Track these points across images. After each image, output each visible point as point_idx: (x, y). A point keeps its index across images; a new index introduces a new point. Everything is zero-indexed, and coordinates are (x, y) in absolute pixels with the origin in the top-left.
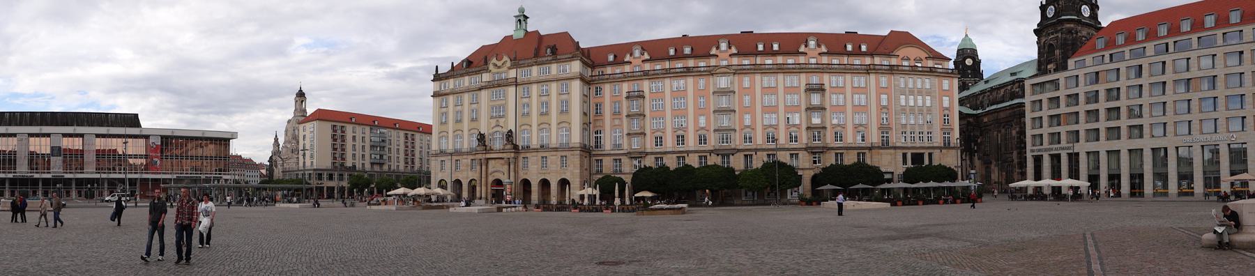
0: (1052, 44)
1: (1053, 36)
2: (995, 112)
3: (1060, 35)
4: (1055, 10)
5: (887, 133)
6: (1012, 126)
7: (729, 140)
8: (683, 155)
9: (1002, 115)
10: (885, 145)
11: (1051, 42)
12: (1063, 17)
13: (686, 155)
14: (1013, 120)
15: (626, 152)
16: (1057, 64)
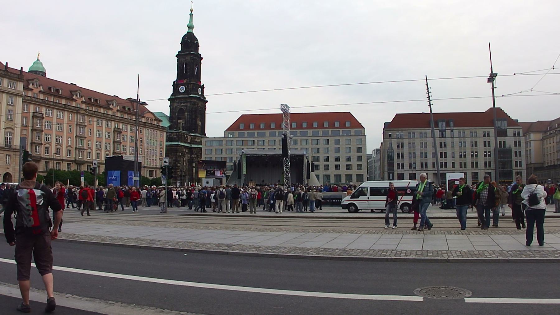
1: (184, 104)
3: (189, 104)
4: (186, 89)
7: (82, 155)
11: (182, 107)
12: (192, 95)
16: (185, 121)
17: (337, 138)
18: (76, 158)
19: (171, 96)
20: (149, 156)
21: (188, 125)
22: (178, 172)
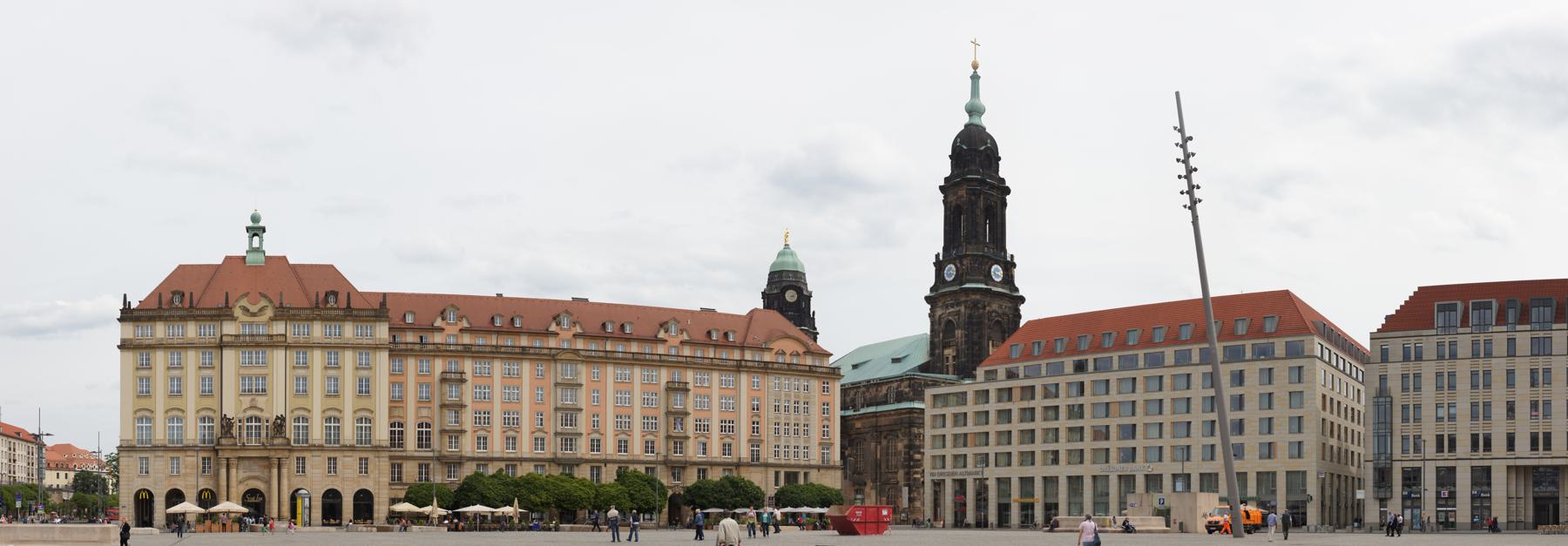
0: (950, 321)
1: (952, 310)
2: (873, 417)
3: (962, 309)
4: (957, 271)
5: (758, 446)
6: (898, 437)
8: (515, 463)
9: (883, 421)
10: (756, 462)
11: (950, 318)
12: (967, 286)
13: (518, 464)
14: (900, 430)
15: (436, 454)
16: (958, 351)
17: (1237, 367)
18: (555, 454)
19: (932, 290)
20: (783, 439)
21: (963, 360)
22: (917, 473)
